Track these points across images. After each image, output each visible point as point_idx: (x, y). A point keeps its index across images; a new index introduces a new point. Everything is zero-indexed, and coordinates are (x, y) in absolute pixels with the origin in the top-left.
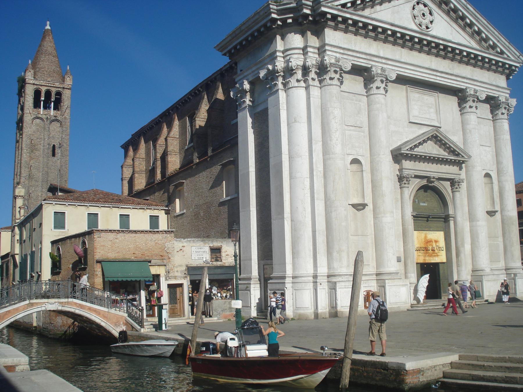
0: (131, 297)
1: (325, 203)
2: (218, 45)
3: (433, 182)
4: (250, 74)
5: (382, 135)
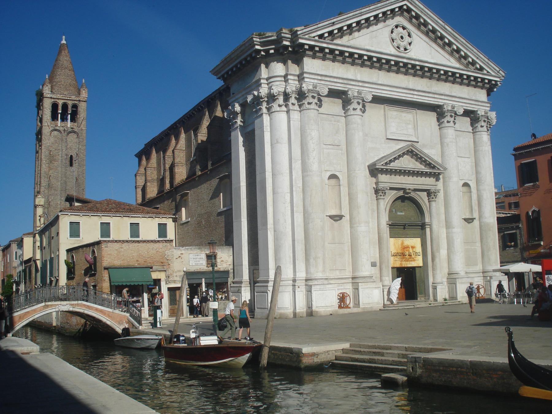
0: (135, 299)
1: (304, 215)
2: (213, 70)
3: (408, 193)
4: (241, 97)
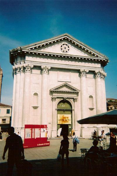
3: (65, 99)
5: (45, 85)
